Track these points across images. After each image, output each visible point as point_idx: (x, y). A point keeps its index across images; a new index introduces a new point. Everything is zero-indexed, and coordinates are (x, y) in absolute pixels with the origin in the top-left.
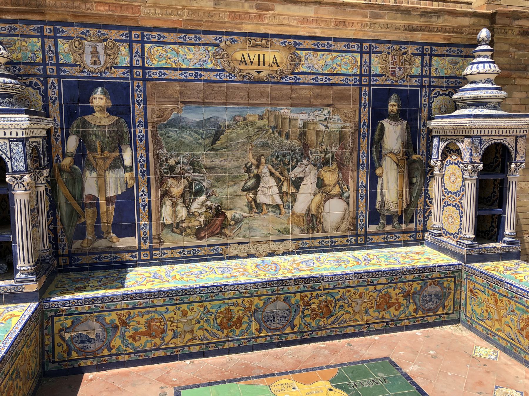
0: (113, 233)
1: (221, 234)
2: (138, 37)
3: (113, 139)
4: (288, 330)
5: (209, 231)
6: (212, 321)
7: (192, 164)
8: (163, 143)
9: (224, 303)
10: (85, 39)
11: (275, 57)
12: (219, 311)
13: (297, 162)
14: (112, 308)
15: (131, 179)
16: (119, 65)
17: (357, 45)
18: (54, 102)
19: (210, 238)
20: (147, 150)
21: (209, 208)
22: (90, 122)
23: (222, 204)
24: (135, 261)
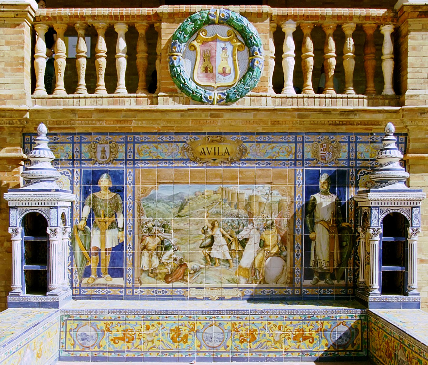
0: (109, 273)
1: (183, 280)
2: (131, 140)
3: (112, 209)
4: (222, 349)
5: (174, 277)
6: (166, 335)
7: (164, 226)
8: (145, 212)
9: (175, 323)
10: (98, 143)
11: (227, 149)
12: (171, 329)
13: (244, 226)
14: (102, 318)
15: (122, 236)
16: (118, 159)
17: (292, 137)
18: (77, 184)
19: (175, 283)
20: (133, 217)
21: (175, 260)
22: (98, 197)
23: (184, 257)
24: (122, 296)
